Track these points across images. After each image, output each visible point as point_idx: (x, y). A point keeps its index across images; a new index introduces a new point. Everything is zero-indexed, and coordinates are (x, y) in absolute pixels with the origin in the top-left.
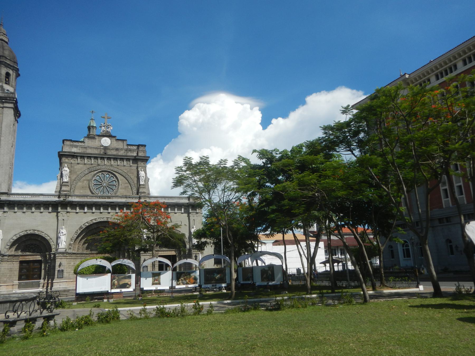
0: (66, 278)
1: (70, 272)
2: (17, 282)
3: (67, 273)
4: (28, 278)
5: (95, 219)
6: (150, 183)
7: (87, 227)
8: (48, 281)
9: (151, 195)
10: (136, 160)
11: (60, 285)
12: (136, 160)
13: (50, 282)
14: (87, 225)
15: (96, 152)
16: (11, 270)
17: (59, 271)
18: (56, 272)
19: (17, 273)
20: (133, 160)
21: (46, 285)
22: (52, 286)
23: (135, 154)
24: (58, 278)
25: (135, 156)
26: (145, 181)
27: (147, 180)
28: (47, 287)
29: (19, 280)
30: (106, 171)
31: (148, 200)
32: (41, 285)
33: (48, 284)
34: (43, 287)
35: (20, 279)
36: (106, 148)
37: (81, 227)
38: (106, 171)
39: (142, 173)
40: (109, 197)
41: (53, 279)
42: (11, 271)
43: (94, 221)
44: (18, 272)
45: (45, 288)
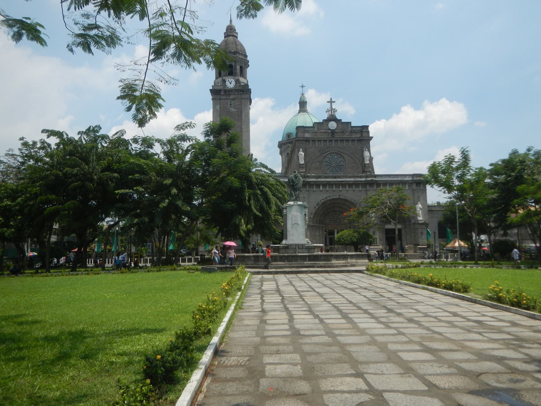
5: (329, 197)
6: (374, 162)
7: (323, 203)
9: (376, 173)
10: (360, 140)
12: (360, 140)
14: (323, 201)
15: (325, 136)
20: (358, 140)
23: (359, 135)
25: (359, 137)
26: (369, 160)
27: (371, 159)
30: (333, 153)
31: (374, 179)
36: (333, 132)
37: (318, 204)
38: (333, 153)
39: (366, 154)
40: (339, 177)
43: (328, 198)
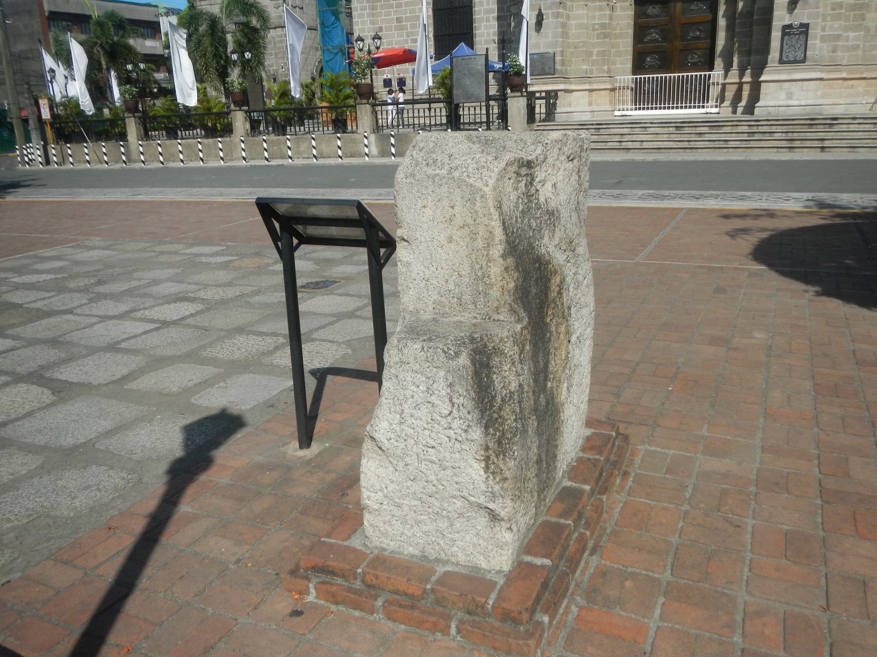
0: (818, 64)
1: (838, 37)
2: (627, 78)
3: (823, 39)
4: (665, 66)
8: (741, 75)
11: (790, 96)
13: (747, 78)
16: (605, 32)
17: (787, 30)
18: (776, 35)
19: (626, 44)
21: (729, 94)
22: (755, 97)
24: (781, 61)
28: (737, 98)
29: (634, 73)
32: (714, 92)
33: (740, 85)
34: (722, 98)
35: (638, 66)
41: (759, 70)
42: (605, 36)
44: (630, 40)
45: (727, 103)
